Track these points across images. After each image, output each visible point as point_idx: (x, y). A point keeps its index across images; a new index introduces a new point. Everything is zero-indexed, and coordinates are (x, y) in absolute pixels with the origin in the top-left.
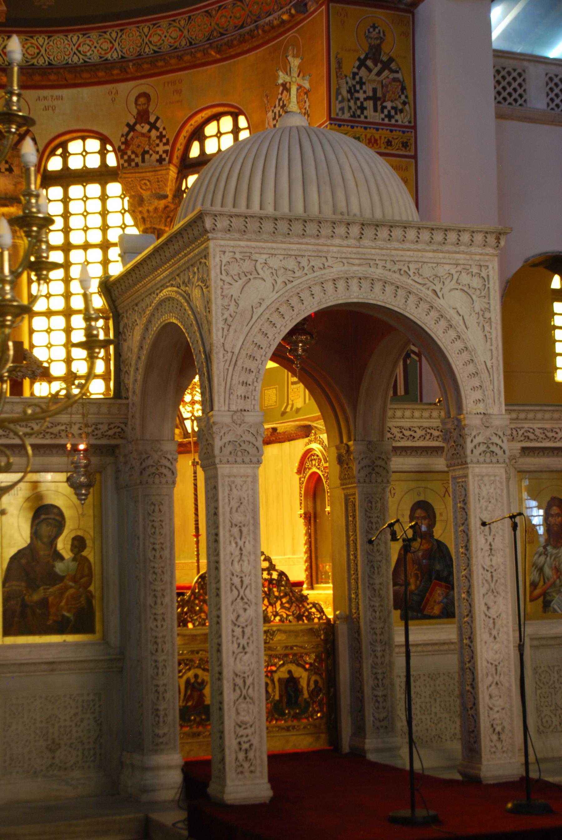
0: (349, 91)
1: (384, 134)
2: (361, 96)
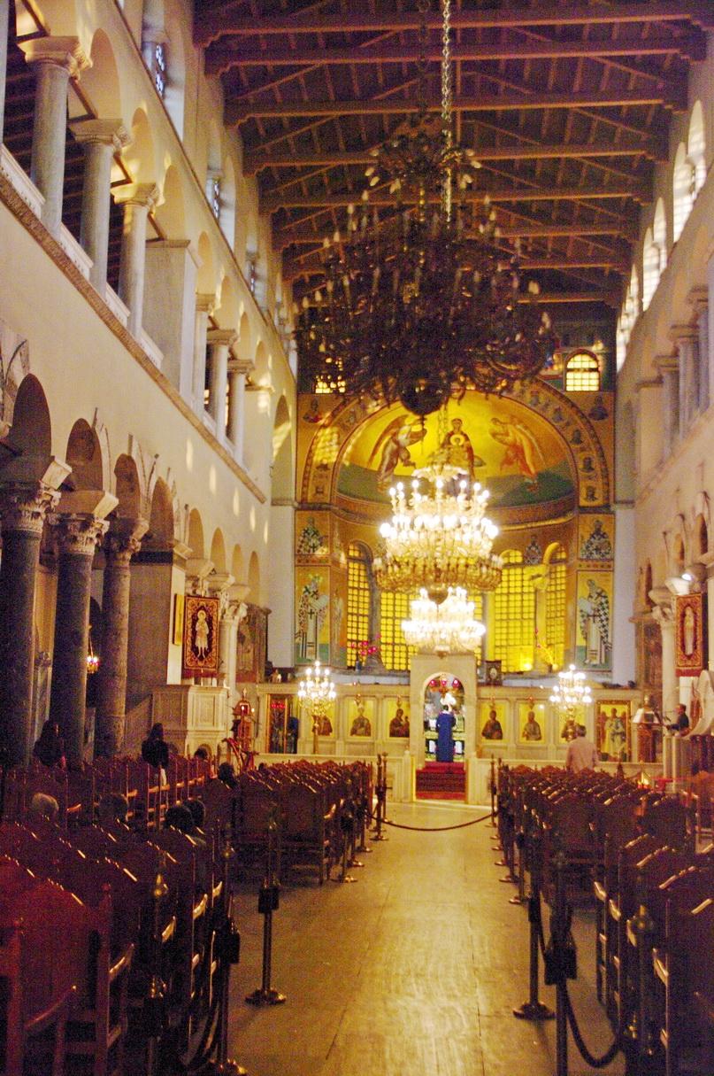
1: (600, 563)
2: (591, 549)
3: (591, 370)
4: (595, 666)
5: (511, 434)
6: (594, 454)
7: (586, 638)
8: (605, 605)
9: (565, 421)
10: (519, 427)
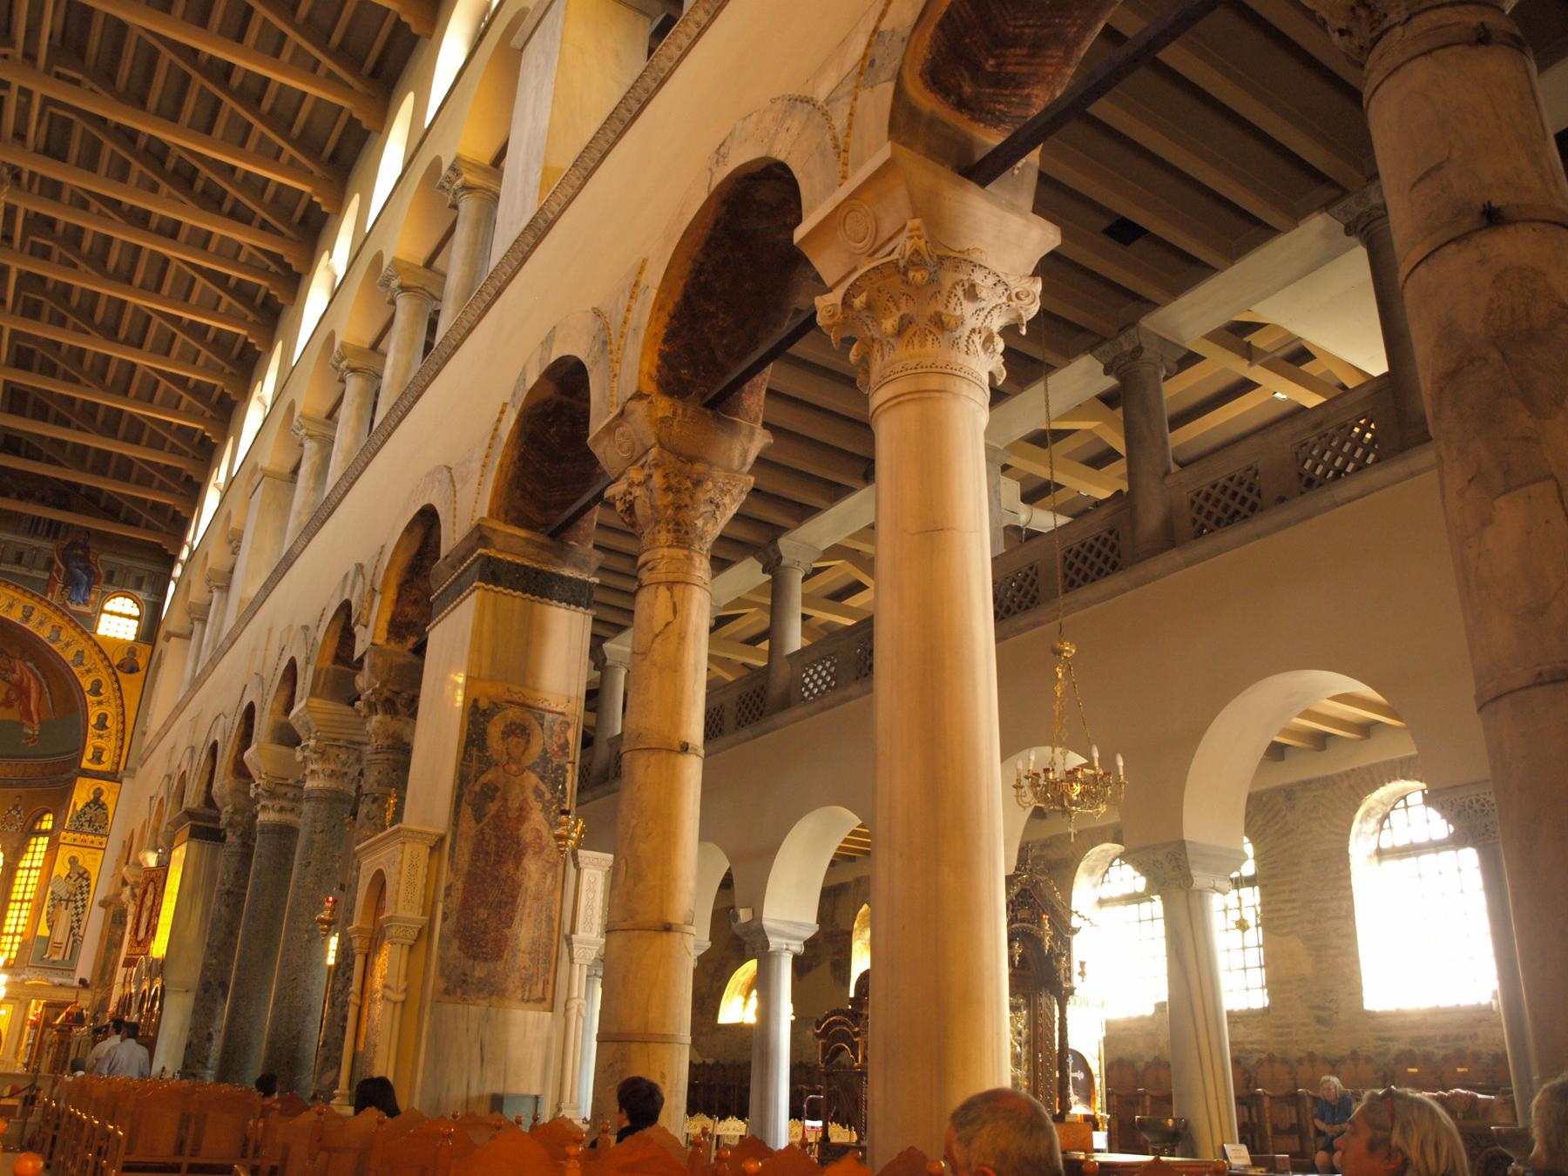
0: (77, 818)
1: (91, 838)
2: (83, 820)
3: (130, 617)
4: (54, 962)
5: (18, 671)
6: (111, 711)
7: (51, 927)
8: (85, 889)
9: (86, 668)
10: (29, 664)
